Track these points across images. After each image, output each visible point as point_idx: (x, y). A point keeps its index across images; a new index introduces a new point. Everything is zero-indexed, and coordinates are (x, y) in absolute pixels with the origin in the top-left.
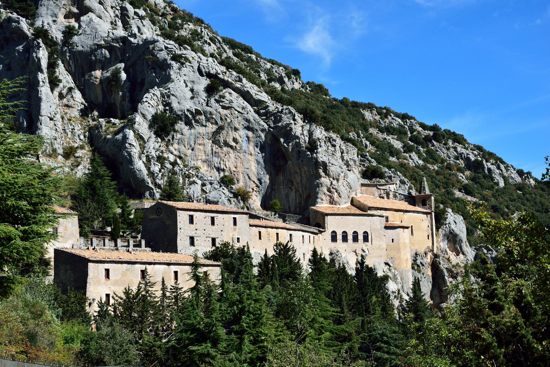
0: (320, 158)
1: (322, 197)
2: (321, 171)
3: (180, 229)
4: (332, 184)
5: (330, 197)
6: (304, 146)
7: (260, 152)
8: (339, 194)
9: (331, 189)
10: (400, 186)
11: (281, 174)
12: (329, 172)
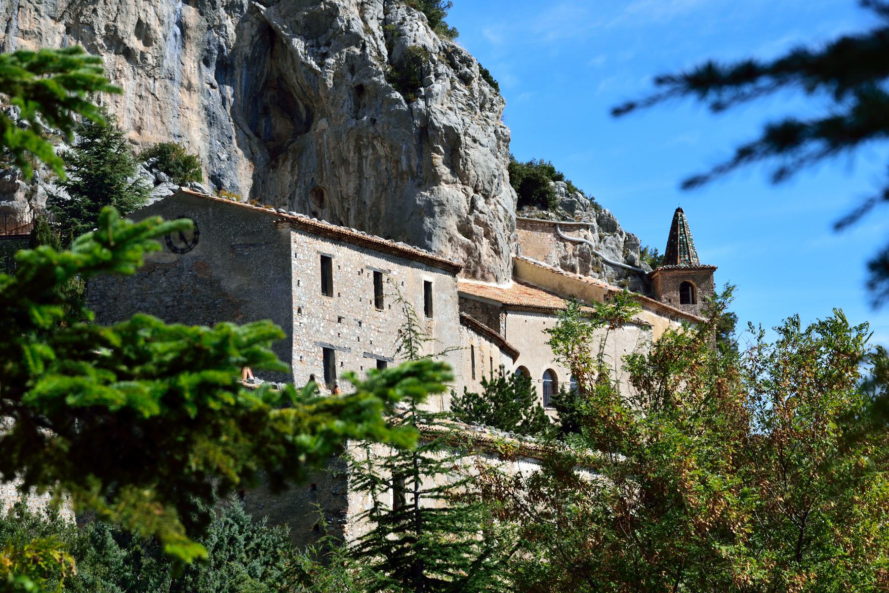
0: (439, 116)
1: (443, 248)
2: (439, 159)
3: (299, 311)
4: (473, 205)
5: (469, 251)
6: (381, 69)
7: (215, 83)
8: (494, 243)
9: (473, 225)
10: (601, 238)
11: (289, 164)
12: (465, 164)
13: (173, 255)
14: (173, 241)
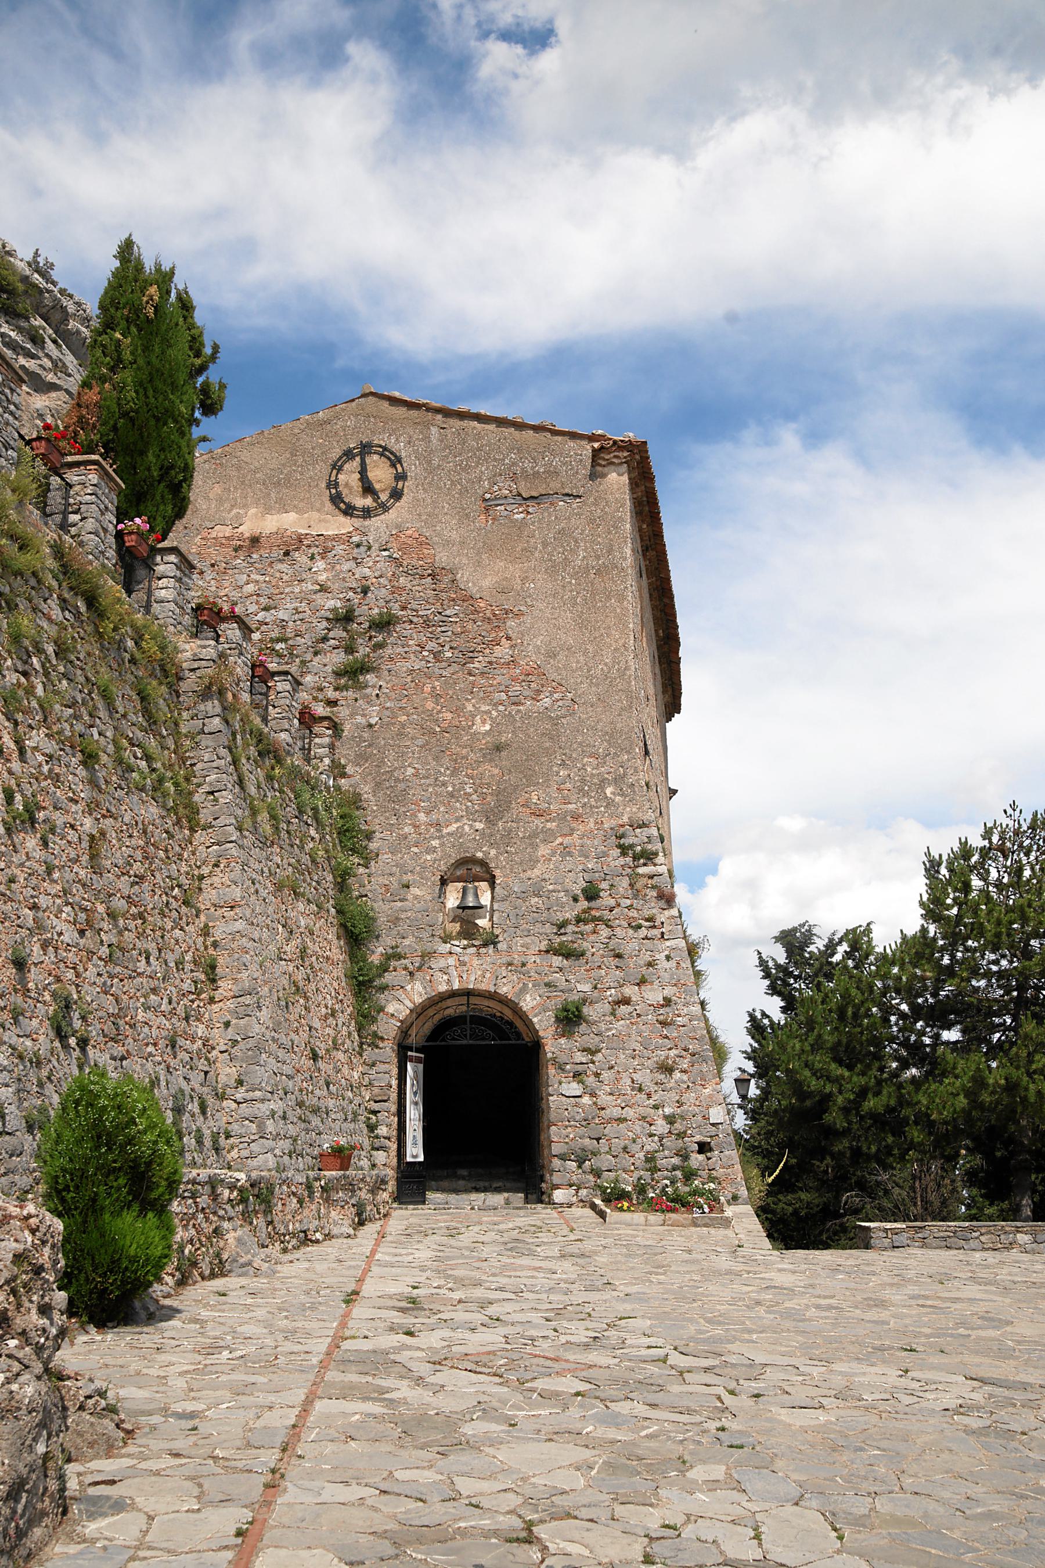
13: (342, 519)
14: (345, 492)
